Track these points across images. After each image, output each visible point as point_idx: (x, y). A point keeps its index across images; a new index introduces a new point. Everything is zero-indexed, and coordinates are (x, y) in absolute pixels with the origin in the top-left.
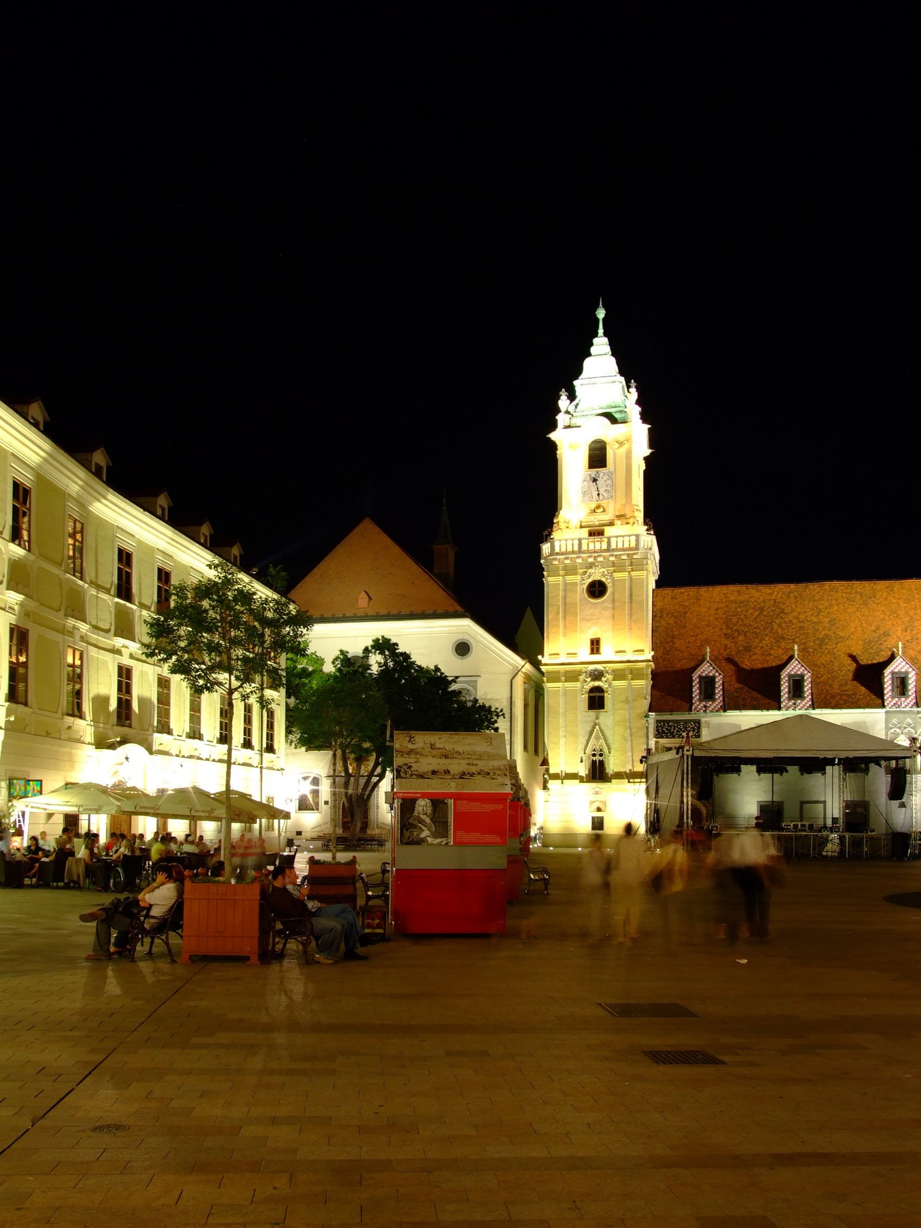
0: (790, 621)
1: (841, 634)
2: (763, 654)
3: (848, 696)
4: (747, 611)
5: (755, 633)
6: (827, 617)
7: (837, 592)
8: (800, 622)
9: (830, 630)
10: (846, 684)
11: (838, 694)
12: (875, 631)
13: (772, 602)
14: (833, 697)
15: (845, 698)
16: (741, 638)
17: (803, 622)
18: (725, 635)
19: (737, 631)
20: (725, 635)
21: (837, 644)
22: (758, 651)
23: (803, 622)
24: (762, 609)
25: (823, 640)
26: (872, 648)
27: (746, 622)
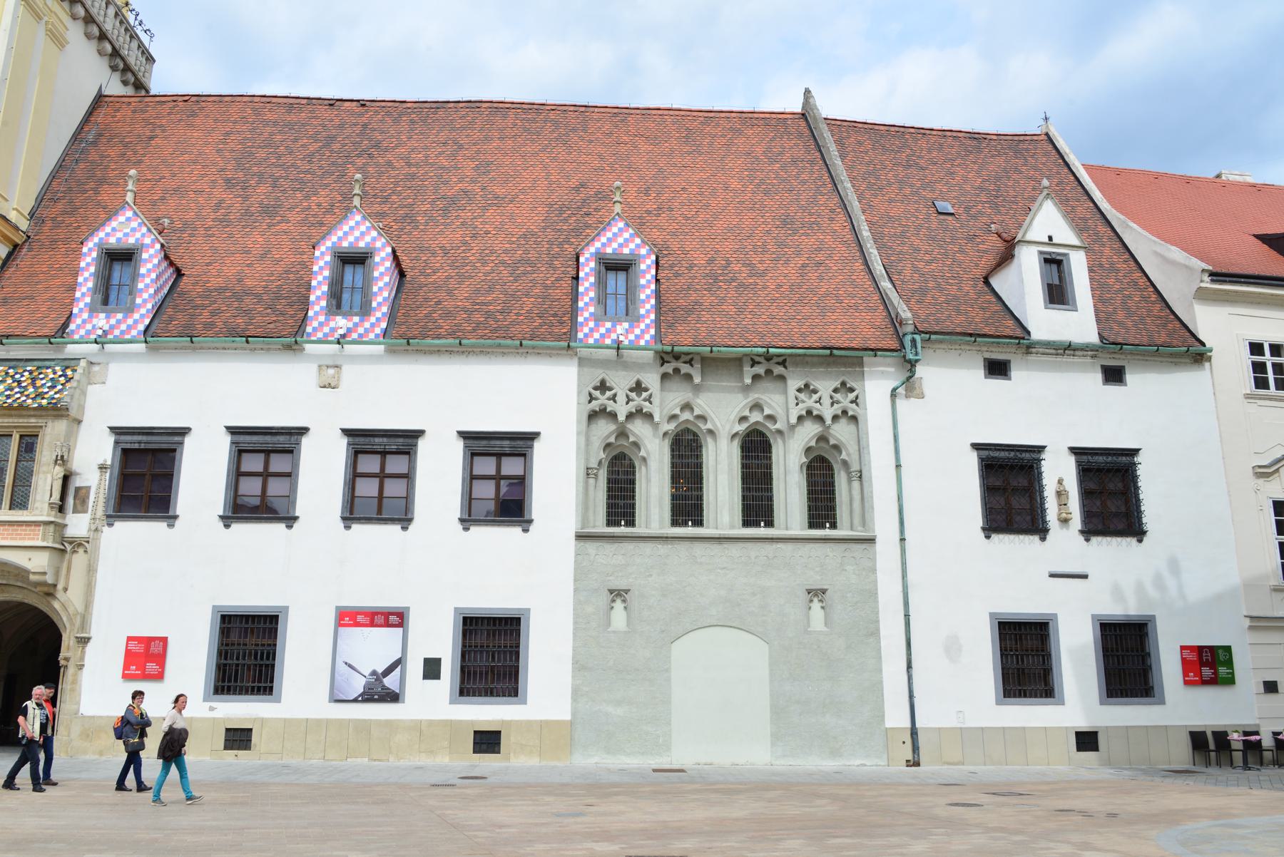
0: (389, 164)
1: (500, 191)
2: (302, 223)
3: (489, 315)
4: (296, 140)
5: (302, 182)
6: (472, 159)
7: (505, 117)
8: (409, 165)
9: (474, 181)
10: (491, 290)
11: (465, 310)
12: (577, 189)
13: (358, 129)
14: (448, 314)
15: (478, 317)
16: (262, 189)
17: (417, 165)
18: (228, 181)
19: (261, 175)
20: (228, 181)
21: (485, 209)
22: (294, 217)
23: (417, 165)
24: (331, 139)
25: (453, 201)
26: (566, 220)
27: (288, 160)
